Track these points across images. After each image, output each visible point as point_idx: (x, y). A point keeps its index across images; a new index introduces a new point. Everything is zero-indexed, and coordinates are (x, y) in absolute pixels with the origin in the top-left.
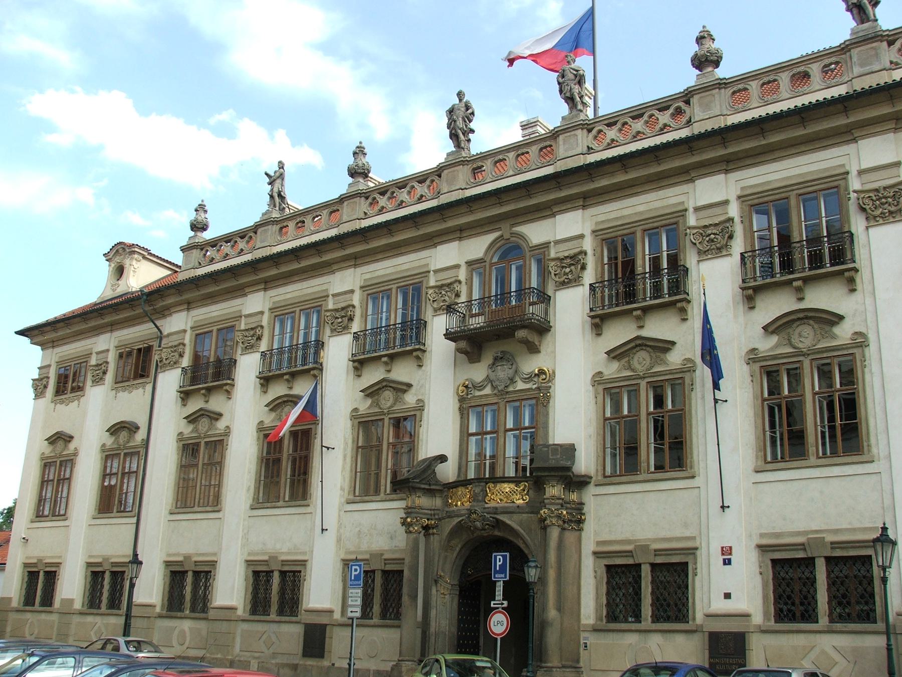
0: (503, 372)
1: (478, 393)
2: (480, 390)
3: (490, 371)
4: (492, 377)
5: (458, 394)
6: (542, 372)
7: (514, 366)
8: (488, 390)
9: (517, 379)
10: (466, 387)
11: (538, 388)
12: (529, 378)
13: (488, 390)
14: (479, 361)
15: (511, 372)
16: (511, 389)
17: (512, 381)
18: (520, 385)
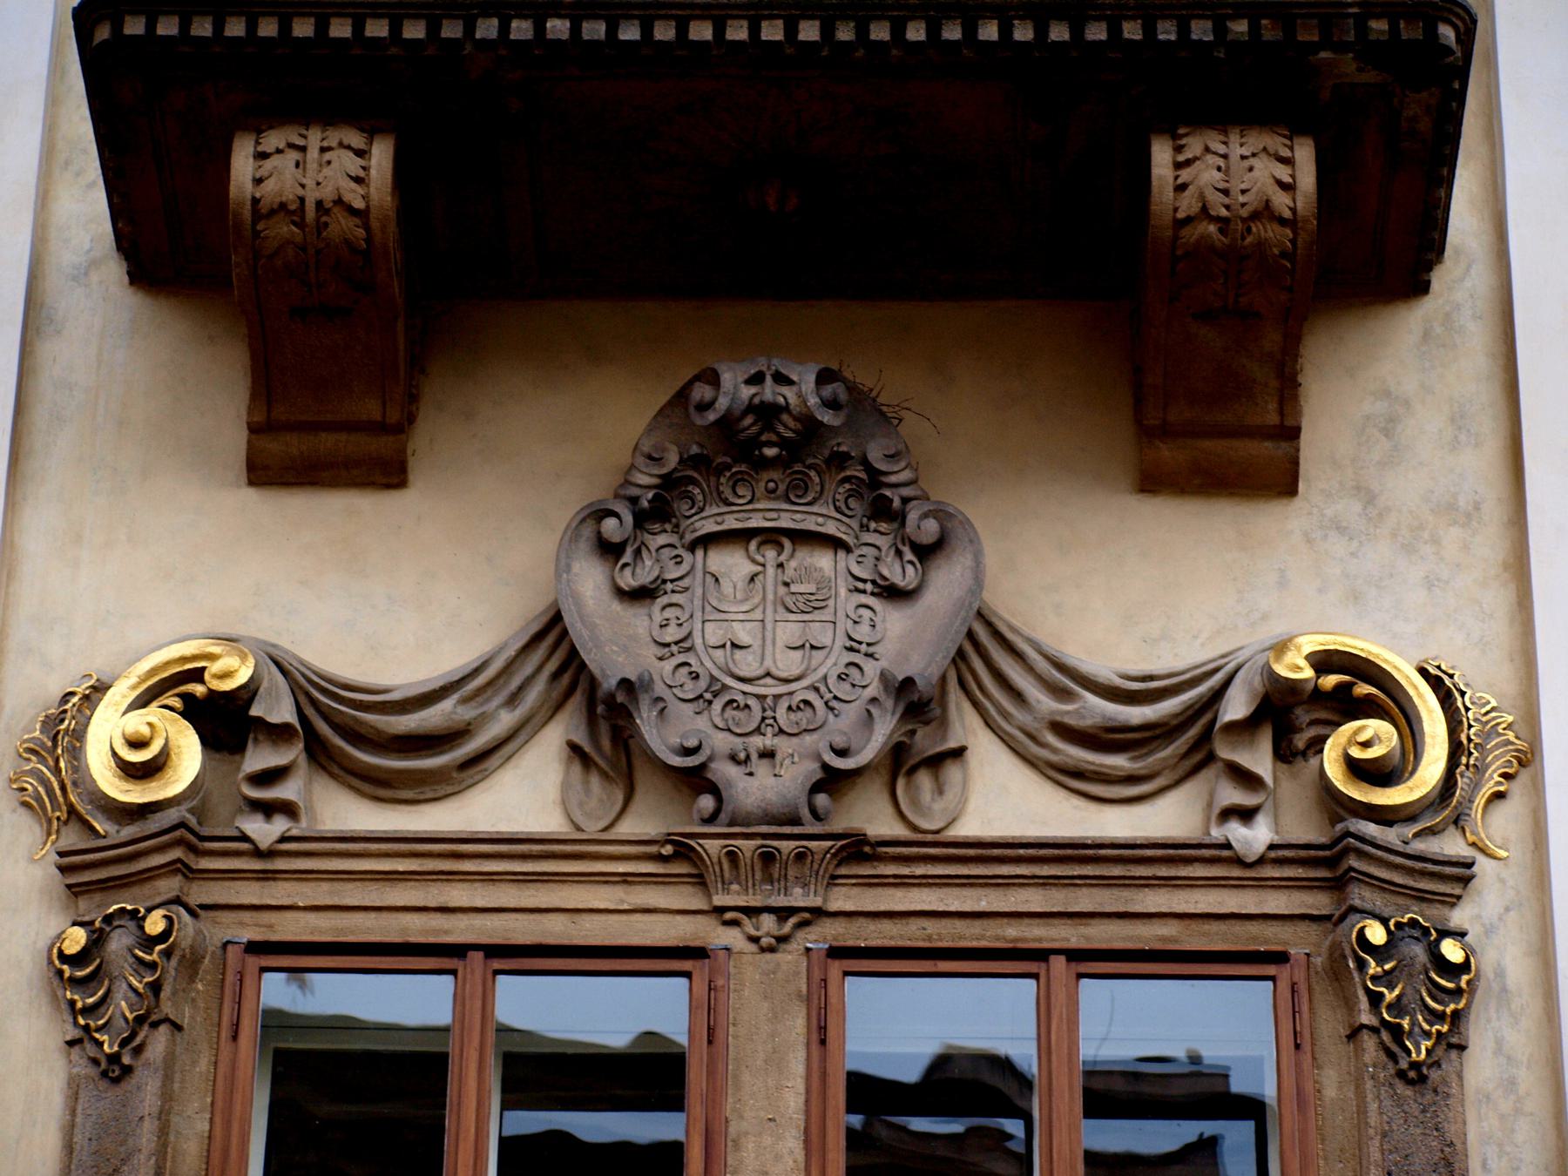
0: (771, 632)
1: (343, 812)
2: (378, 786)
3: (590, 580)
4: (618, 642)
5: (60, 800)
6: (1354, 687)
7: (946, 584)
8: (526, 793)
9: (966, 728)
10: (223, 720)
11: (1331, 863)
12: (1178, 731)
13: (526, 793)
14: (389, 474)
15: (908, 639)
16: (872, 816)
17: (918, 757)
18: (1001, 797)
